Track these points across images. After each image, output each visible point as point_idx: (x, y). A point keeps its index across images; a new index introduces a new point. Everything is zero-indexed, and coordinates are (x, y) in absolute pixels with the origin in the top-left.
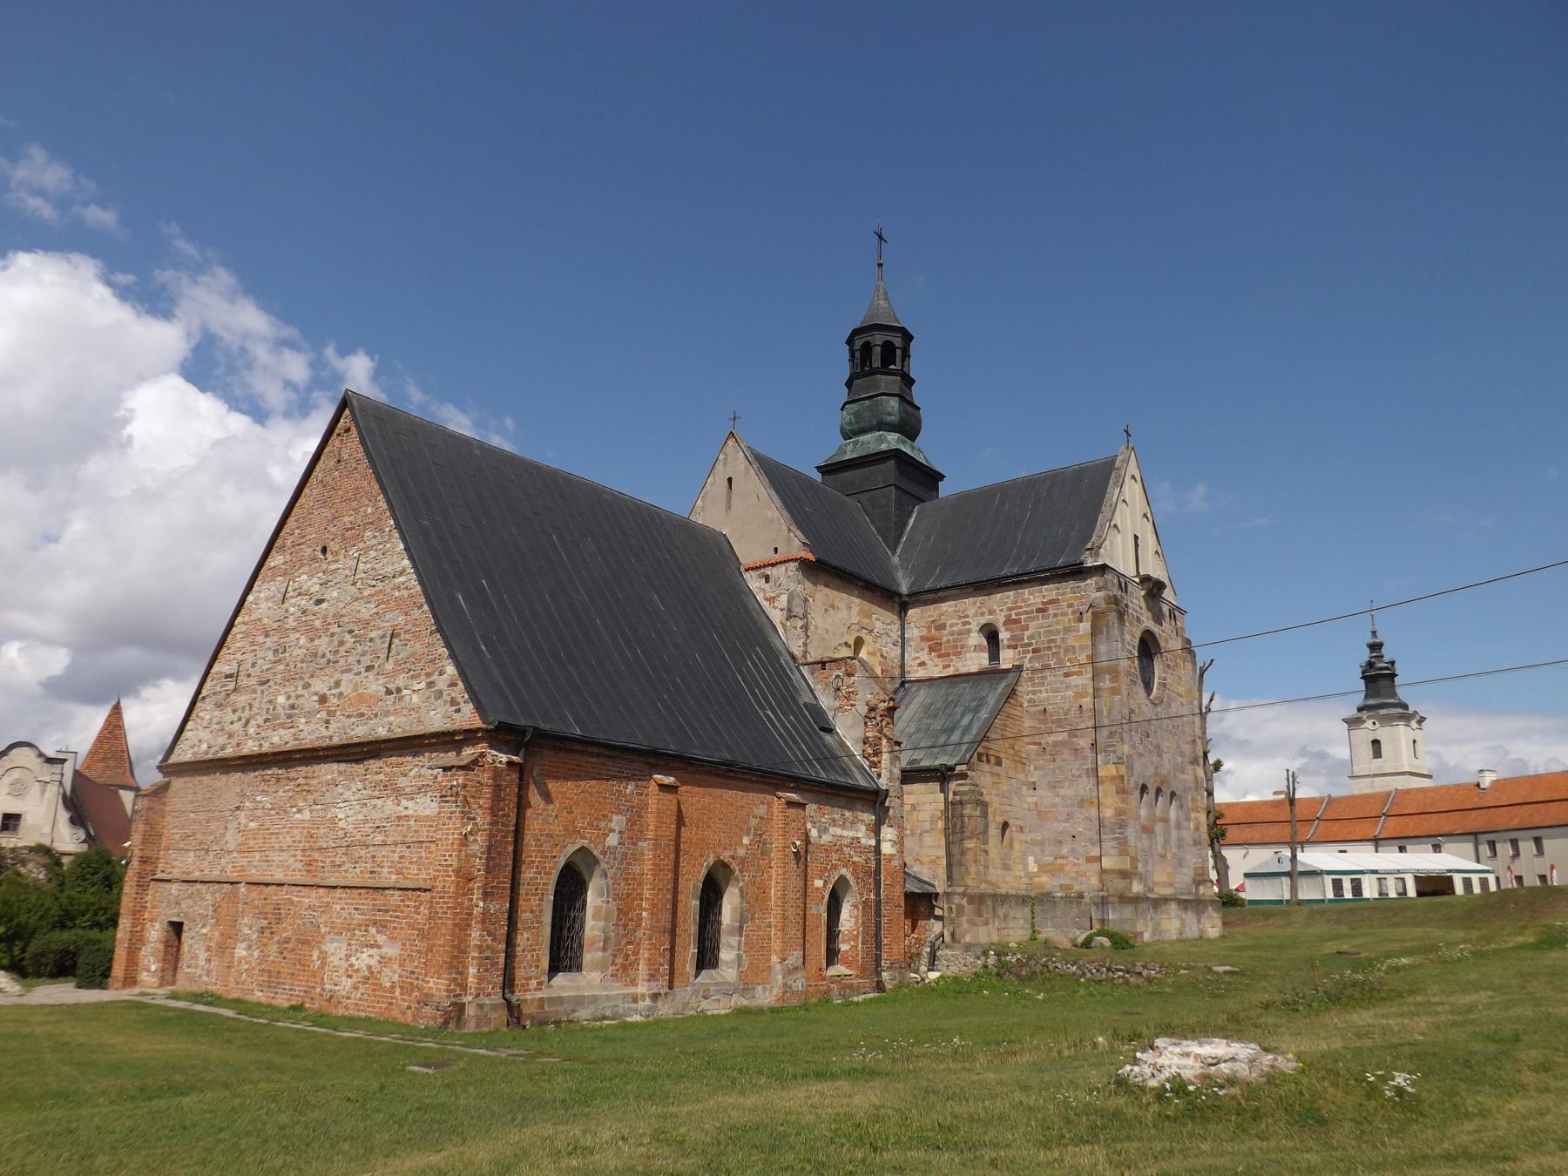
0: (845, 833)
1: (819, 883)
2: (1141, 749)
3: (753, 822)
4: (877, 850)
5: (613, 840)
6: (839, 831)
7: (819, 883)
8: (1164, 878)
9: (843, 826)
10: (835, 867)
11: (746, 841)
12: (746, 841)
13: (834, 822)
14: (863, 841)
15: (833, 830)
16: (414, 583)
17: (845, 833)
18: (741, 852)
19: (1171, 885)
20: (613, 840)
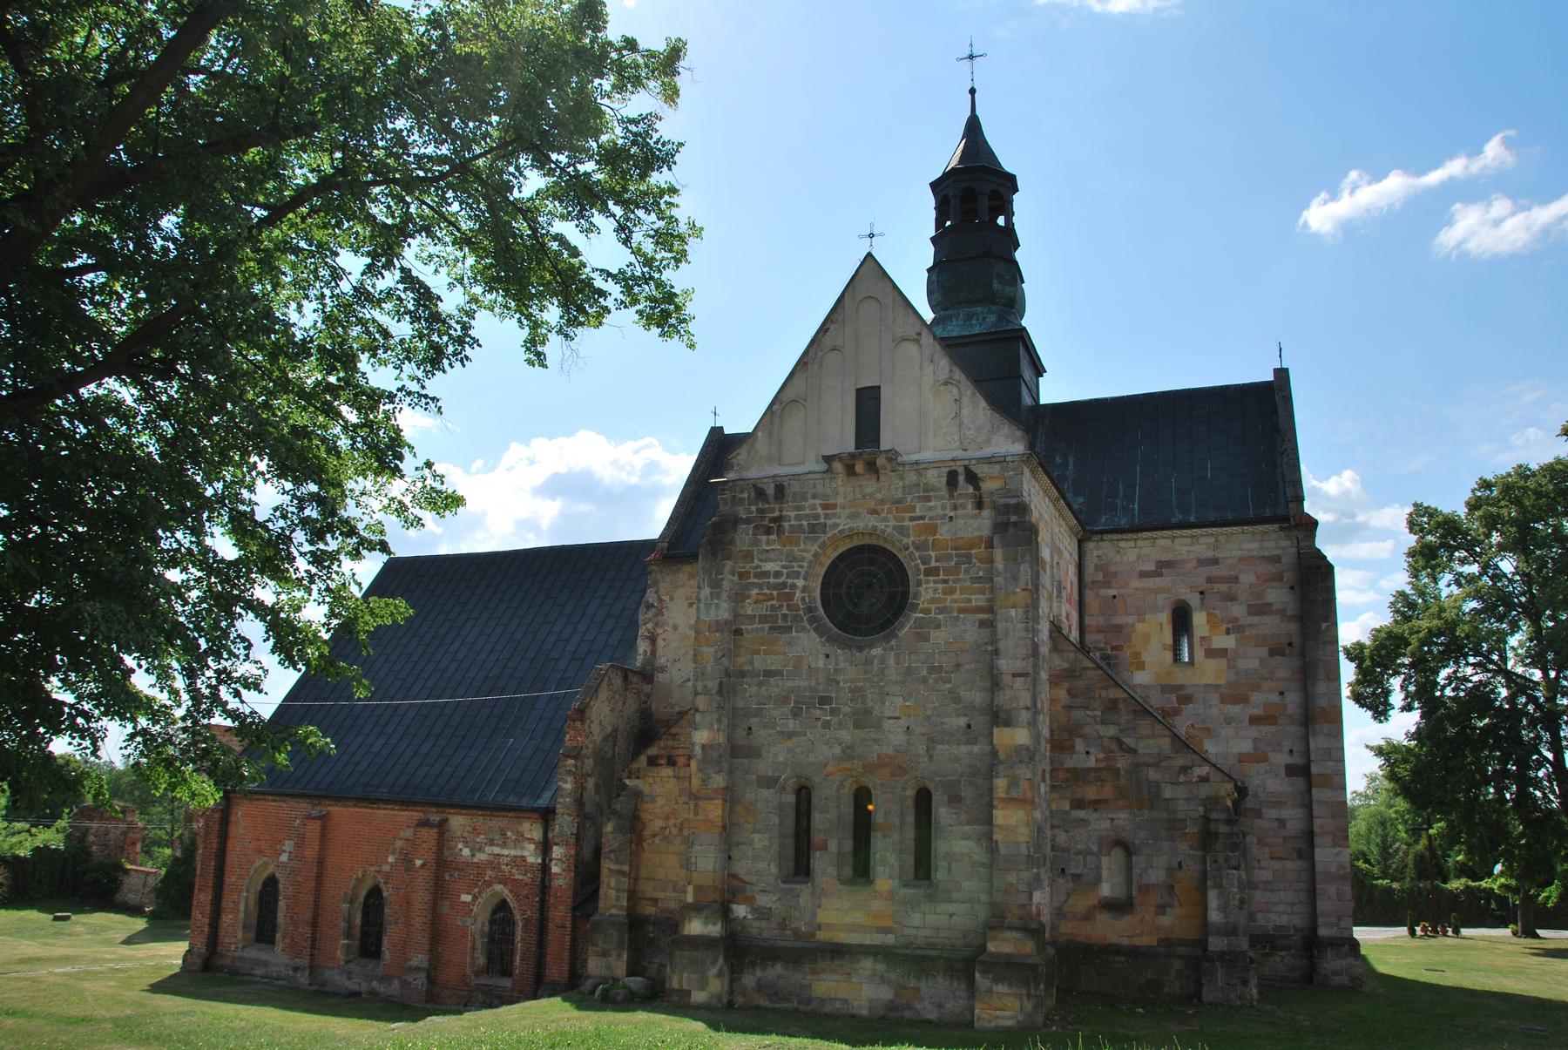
0: (505, 852)
1: (466, 898)
2: (792, 724)
3: (399, 844)
4: (545, 868)
5: (284, 858)
6: (497, 850)
7: (466, 898)
9: (504, 845)
10: (489, 884)
11: (391, 859)
12: (391, 859)
13: (492, 843)
14: (531, 860)
15: (488, 849)
16: (1188, 546)
17: (505, 852)
18: (386, 868)
19: (884, 930)
20: (284, 858)
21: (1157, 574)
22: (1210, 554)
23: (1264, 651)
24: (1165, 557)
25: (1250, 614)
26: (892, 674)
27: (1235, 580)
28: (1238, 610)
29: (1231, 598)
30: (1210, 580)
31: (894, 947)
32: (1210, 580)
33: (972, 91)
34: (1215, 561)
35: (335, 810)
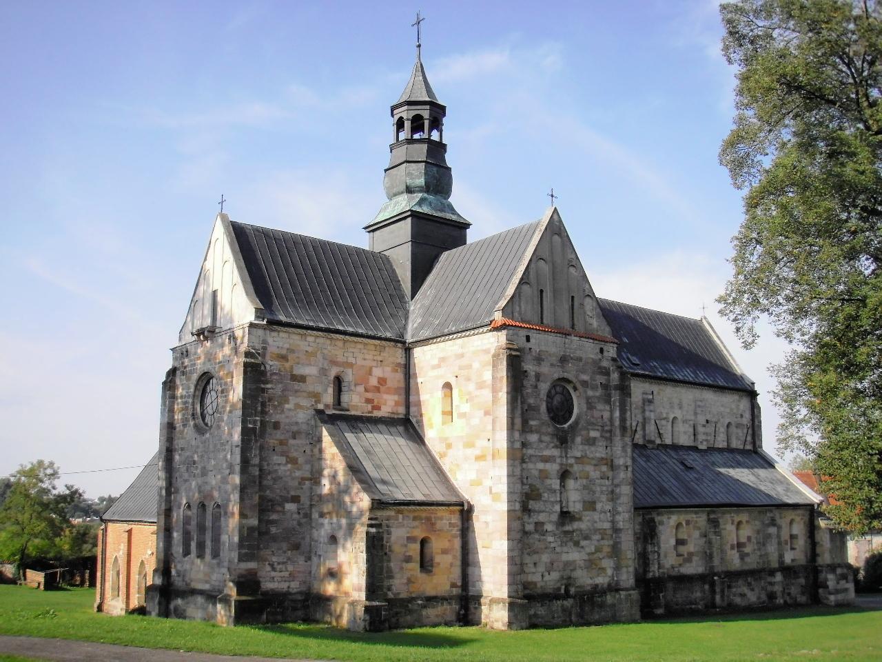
8: (201, 576)
19: (207, 582)
21: (438, 366)
22: (460, 351)
23: (482, 412)
24: (441, 355)
25: (477, 389)
26: (211, 447)
27: (469, 367)
28: (471, 387)
29: (468, 379)
30: (460, 368)
31: (209, 591)
32: (460, 368)
33: (419, 46)
34: (462, 356)
35: (135, 527)
